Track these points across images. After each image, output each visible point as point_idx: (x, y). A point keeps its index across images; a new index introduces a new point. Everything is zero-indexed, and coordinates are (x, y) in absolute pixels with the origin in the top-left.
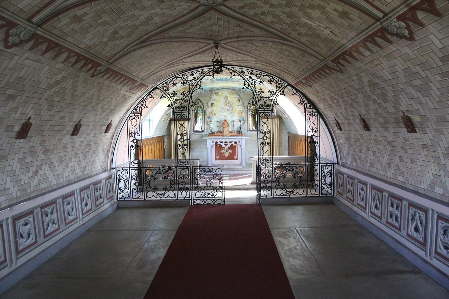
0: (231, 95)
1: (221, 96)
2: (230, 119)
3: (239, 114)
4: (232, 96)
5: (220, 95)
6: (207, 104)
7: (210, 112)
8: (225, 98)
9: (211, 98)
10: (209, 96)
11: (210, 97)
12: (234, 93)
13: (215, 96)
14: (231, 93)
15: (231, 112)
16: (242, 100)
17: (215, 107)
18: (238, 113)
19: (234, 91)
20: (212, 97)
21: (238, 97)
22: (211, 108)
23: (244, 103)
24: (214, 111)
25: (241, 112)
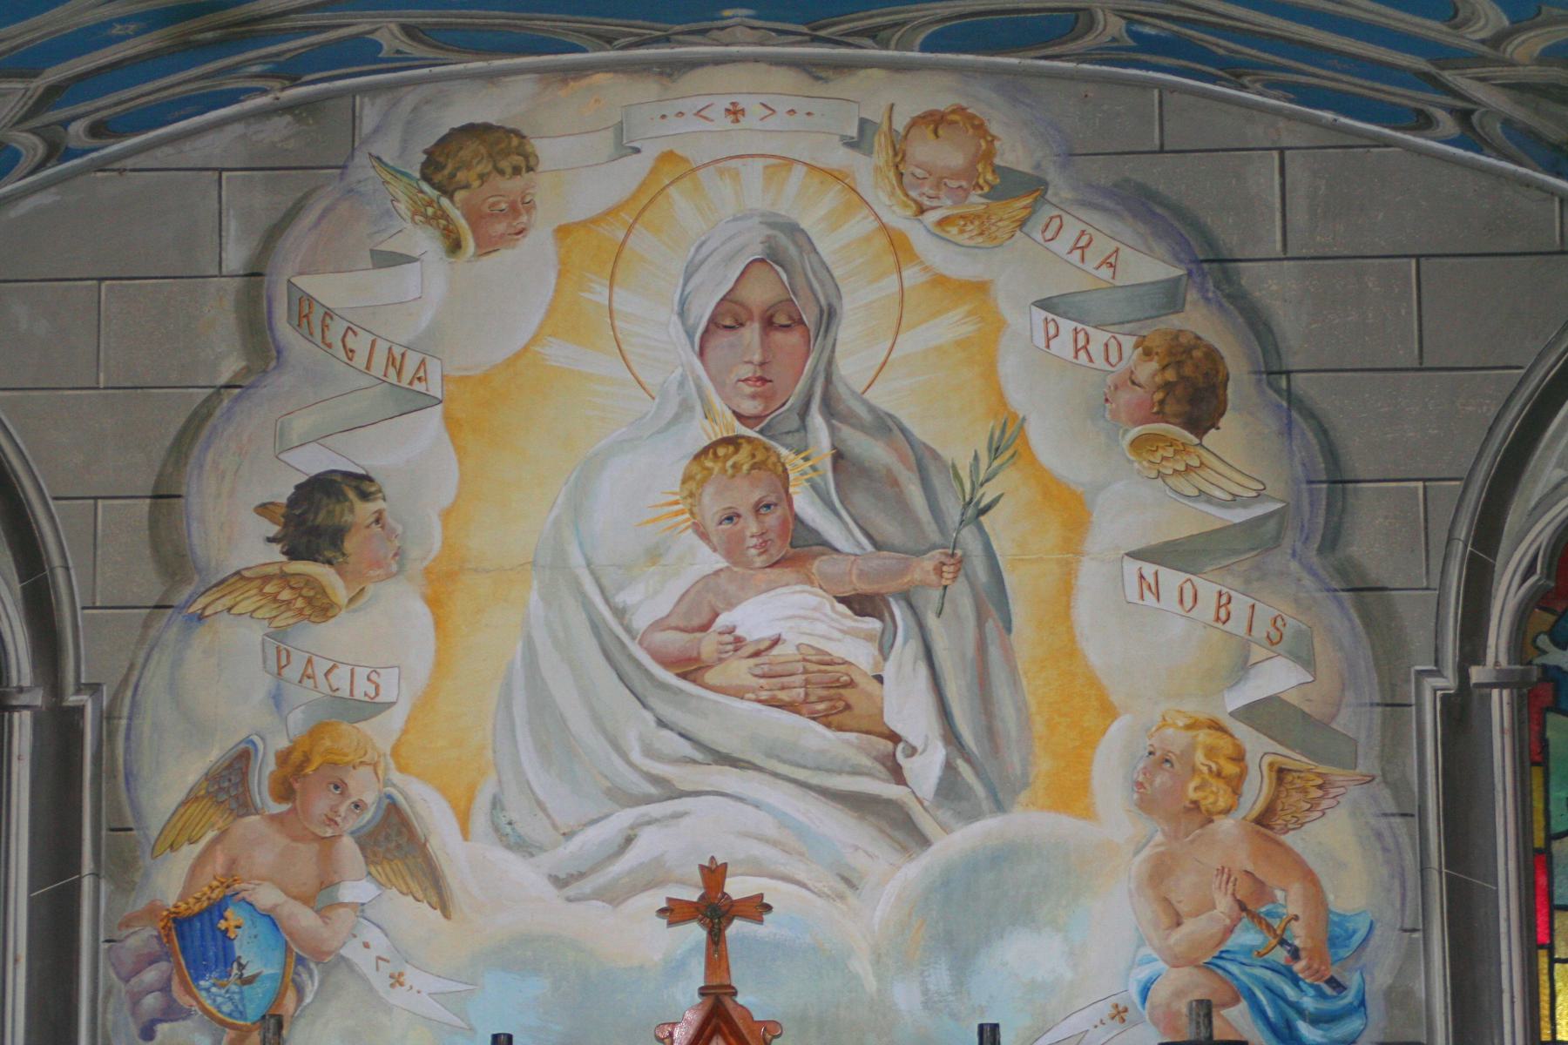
0: (918, 235)
1: (615, 263)
2: (905, 997)
3: (1200, 815)
4: (958, 265)
5: (563, 232)
6: (164, 496)
7: (241, 760)
8: (727, 317)
9: (303, 308)
10: (235, 257)
11: (254, 273)
12: (1015, 152)
13: (424, 242)
14: (929, 152)
15: (926, 768)
16: (1273, 372)
17: (420, 609)
18: (1146, 803)
19: (1010, 84)
20: (325, 288)
21: (1170, 297)
22: (278, 635)
23: (1339, 480)
24: (382, 732)
25: (1257, 746)
